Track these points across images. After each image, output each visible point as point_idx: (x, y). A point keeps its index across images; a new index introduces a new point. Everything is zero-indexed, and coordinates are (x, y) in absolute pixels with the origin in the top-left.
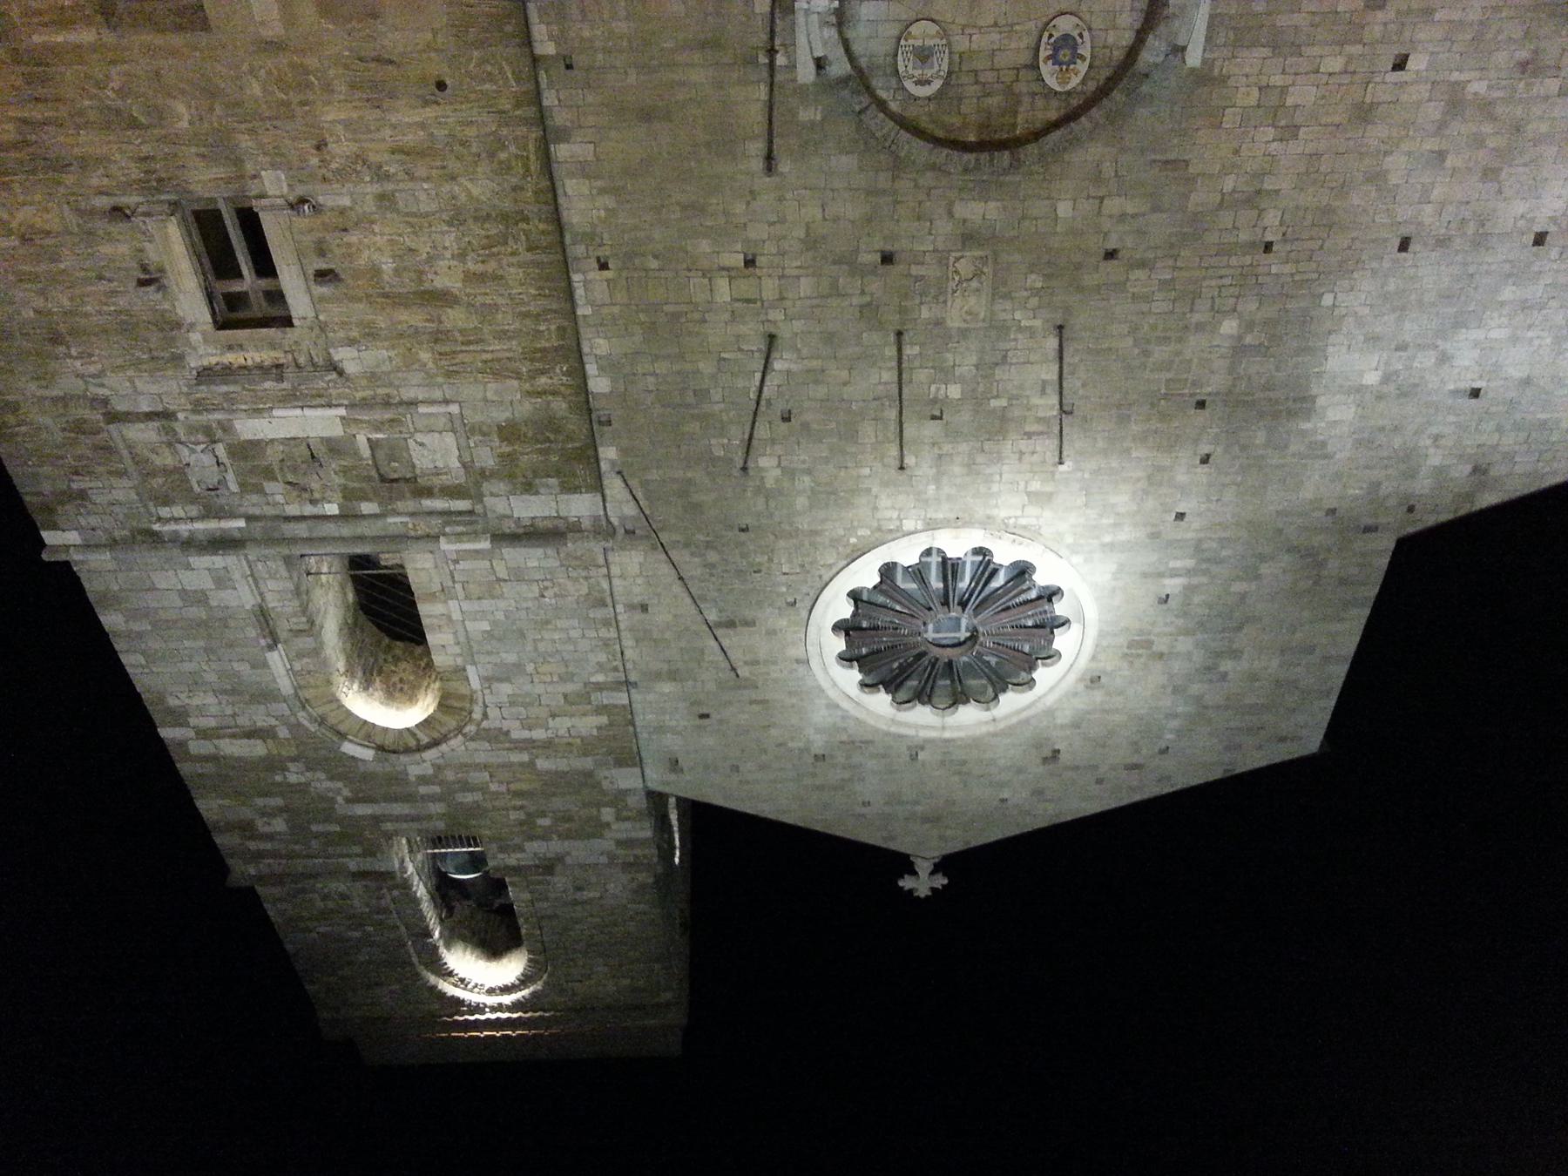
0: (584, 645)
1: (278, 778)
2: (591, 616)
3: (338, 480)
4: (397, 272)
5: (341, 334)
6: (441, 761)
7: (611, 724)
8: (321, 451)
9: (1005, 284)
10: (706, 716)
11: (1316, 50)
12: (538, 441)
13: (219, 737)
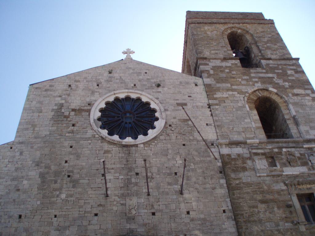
1: (290, 84)
2: (220, 123)
3: (283, 157)
4: (273, 208)
5: (285, 192)
6: (253, 87)
7: (213, 95)
8: (288, 164)
10: (189, 96)
12: (237, 167)
13: (304, 94)
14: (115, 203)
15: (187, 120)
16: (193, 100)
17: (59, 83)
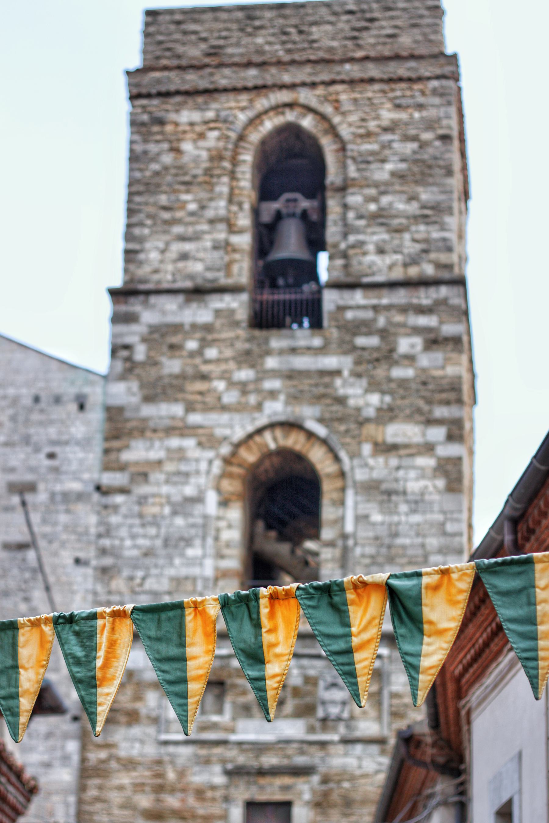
0: (123, 532)
1: (388, 399)
15: (22, 547)
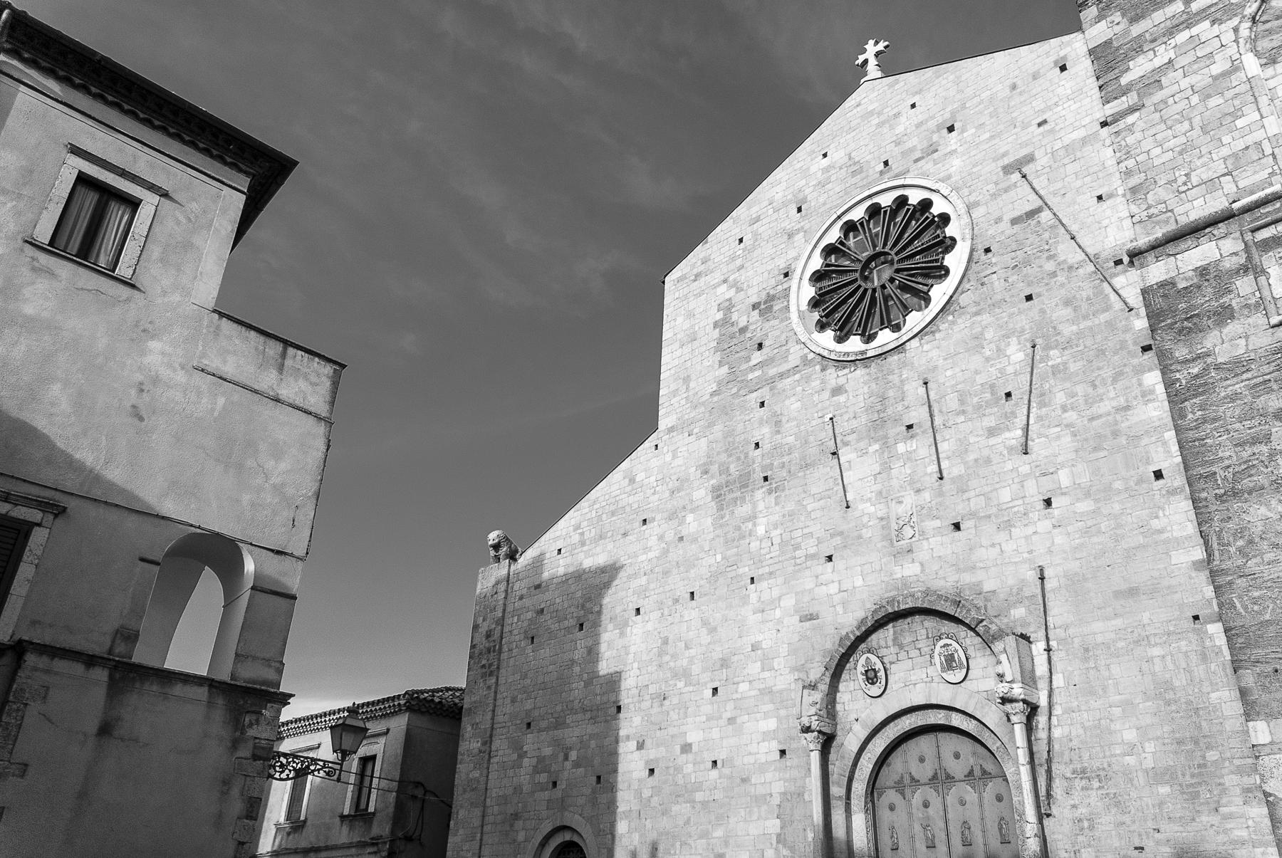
9: (883, 528)
10: (1040, 125)
11: (753, 693)
12: (1197, 315)
14: (865, 519)
15: (1032, 214)
16: (1052, 131)
17: (720, 245)
